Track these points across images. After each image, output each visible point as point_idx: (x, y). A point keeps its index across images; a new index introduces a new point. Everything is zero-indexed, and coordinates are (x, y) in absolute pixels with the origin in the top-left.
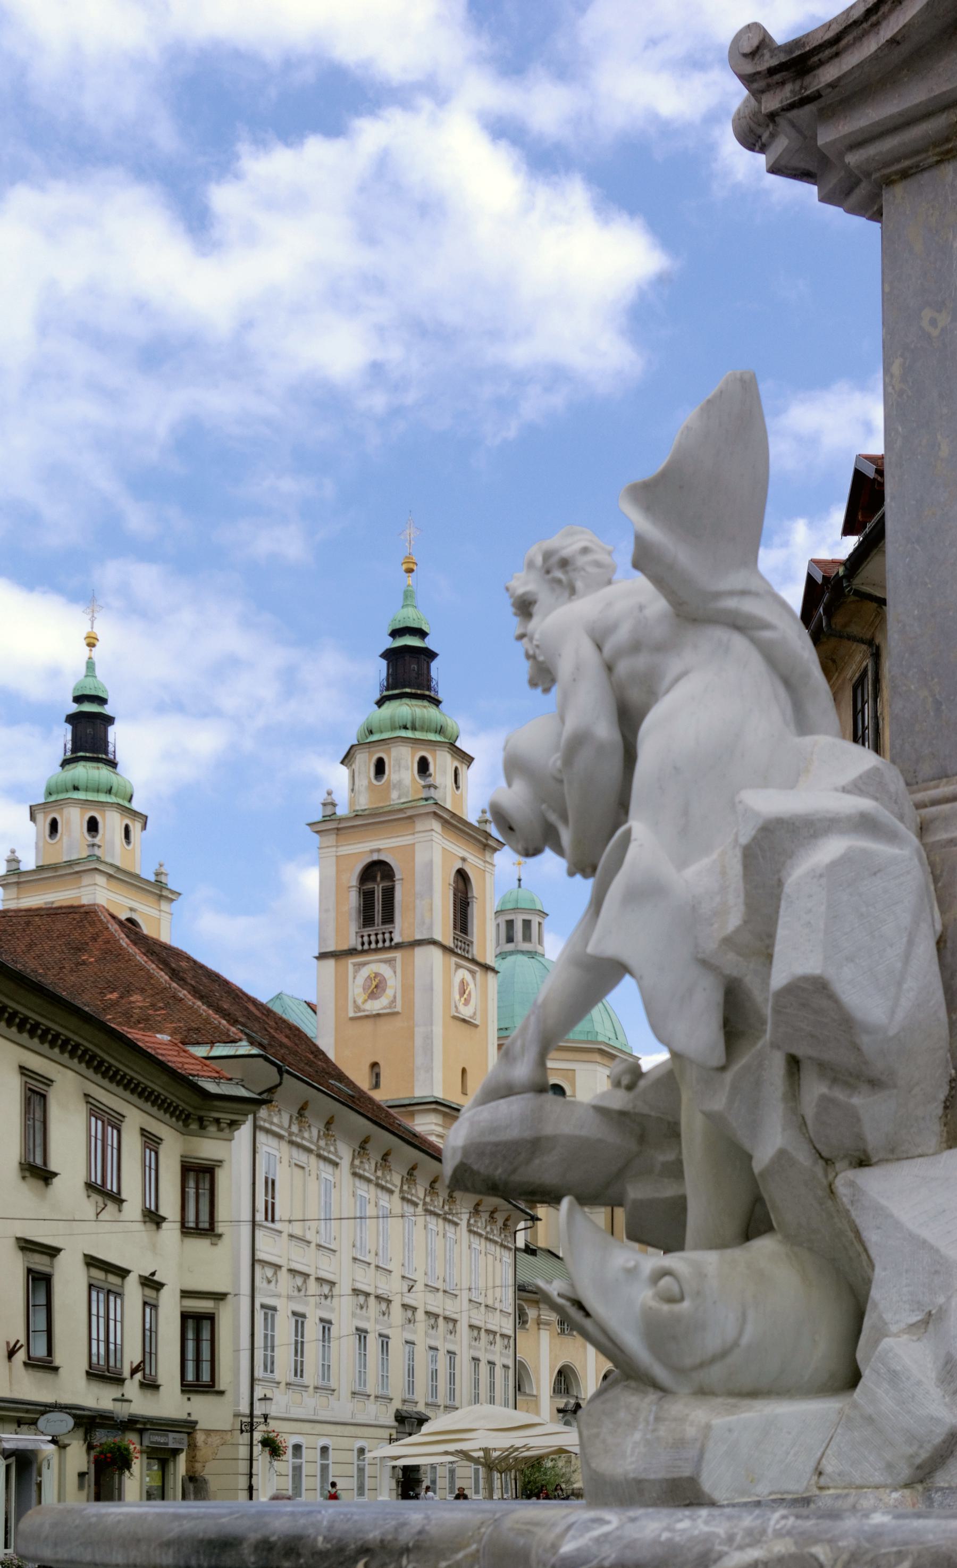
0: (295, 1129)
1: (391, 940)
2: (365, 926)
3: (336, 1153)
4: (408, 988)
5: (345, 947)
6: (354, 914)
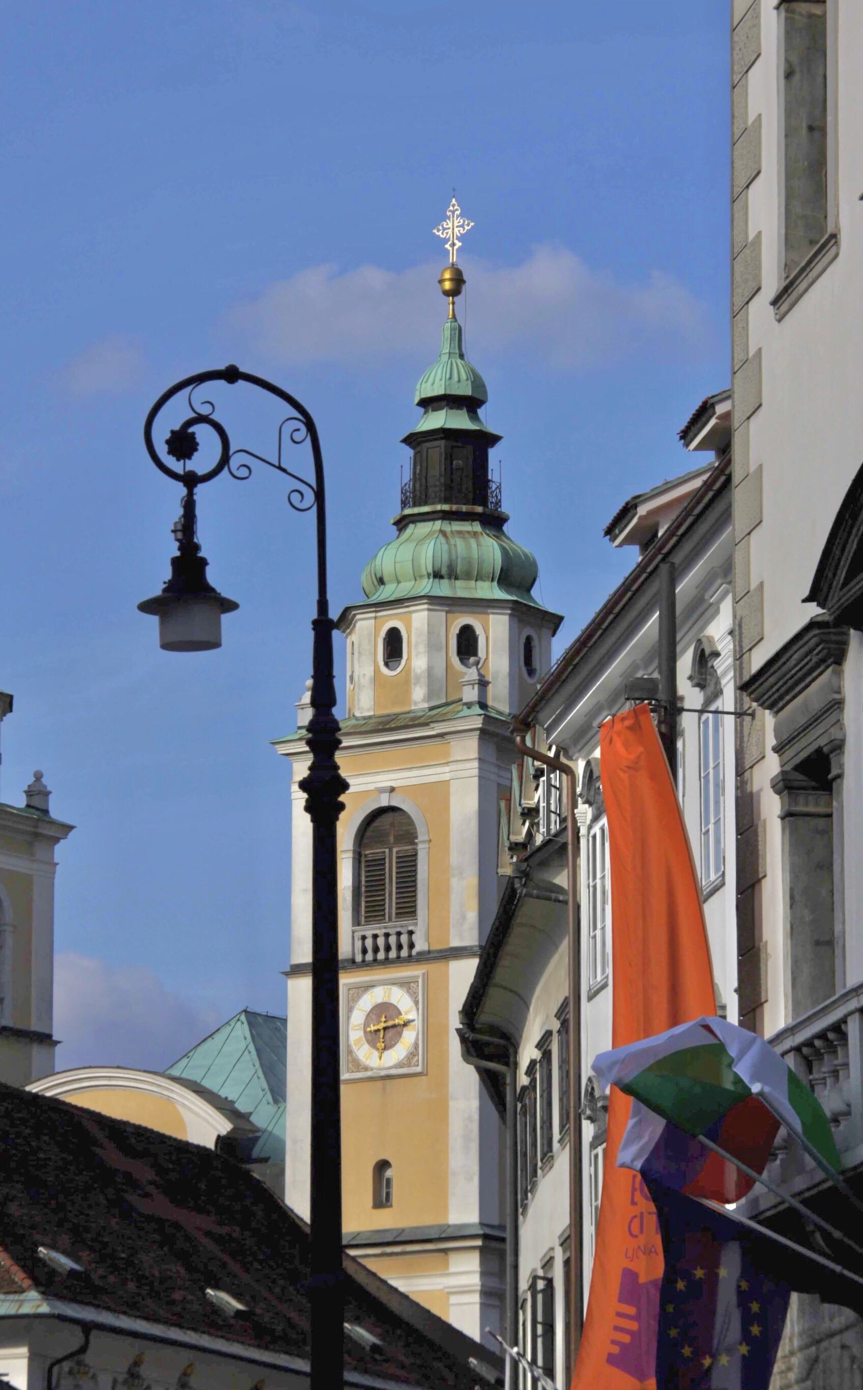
1: (411, 946)
2: (369, 919)
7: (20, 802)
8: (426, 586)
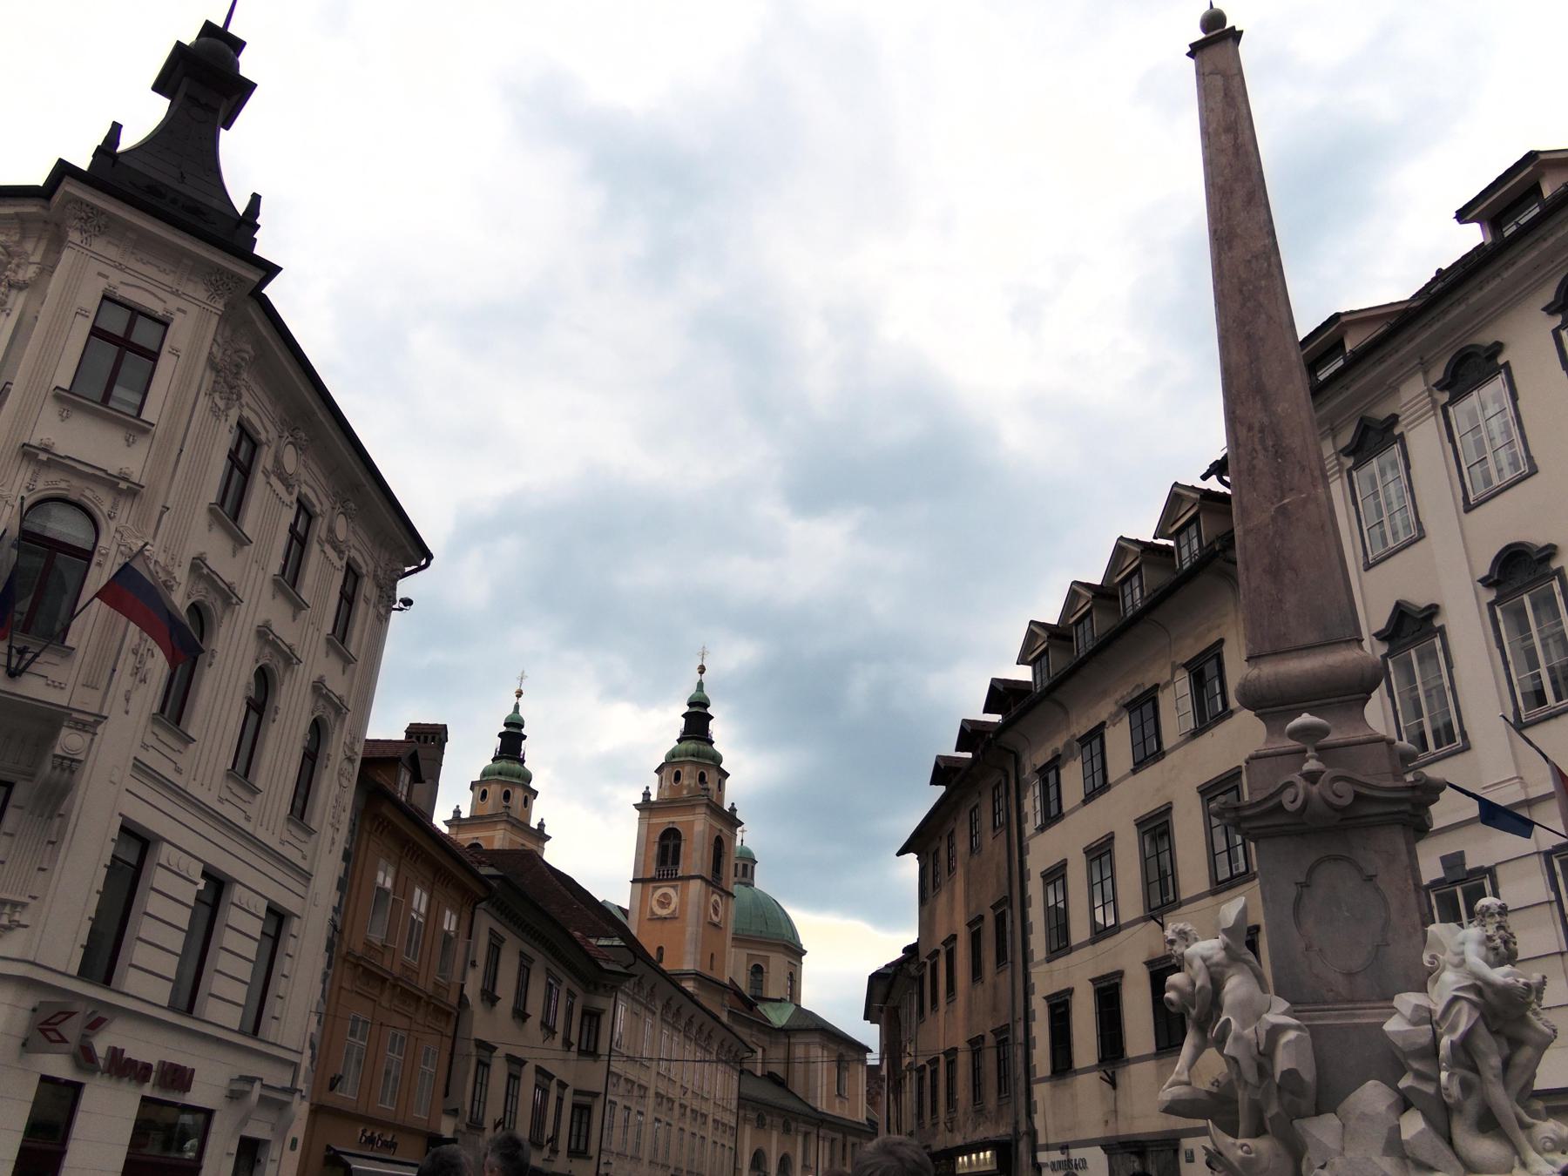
0: (636, 990)
1: (676, 874)
3: (655, 1006)
4: (683, 903)
5: (649, 877)
7: (536, 827)
8: (690, 758)
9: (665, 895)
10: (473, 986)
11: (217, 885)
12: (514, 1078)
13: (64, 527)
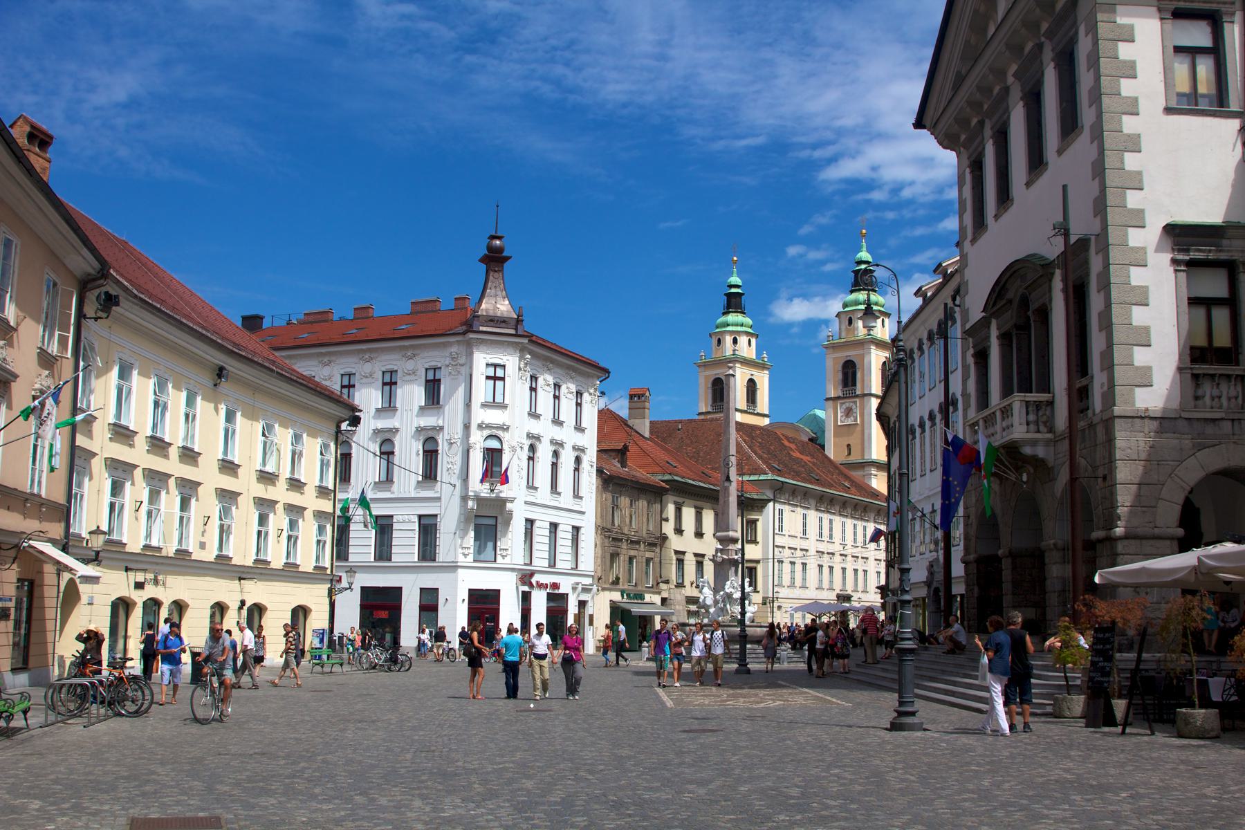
6: (840, 382)
9: (847, 408)
10: (668, 528)
11: (554, 526)
12: (700, 565)
13: (494, 444)
